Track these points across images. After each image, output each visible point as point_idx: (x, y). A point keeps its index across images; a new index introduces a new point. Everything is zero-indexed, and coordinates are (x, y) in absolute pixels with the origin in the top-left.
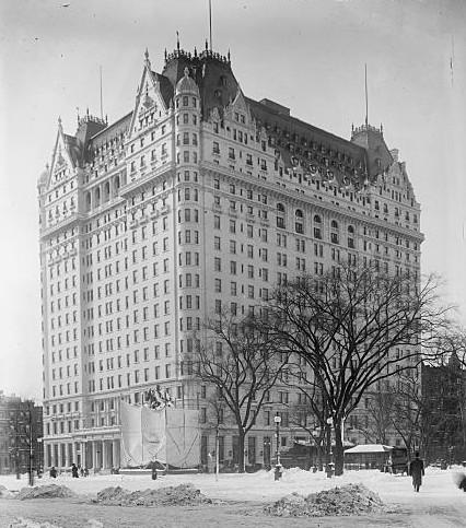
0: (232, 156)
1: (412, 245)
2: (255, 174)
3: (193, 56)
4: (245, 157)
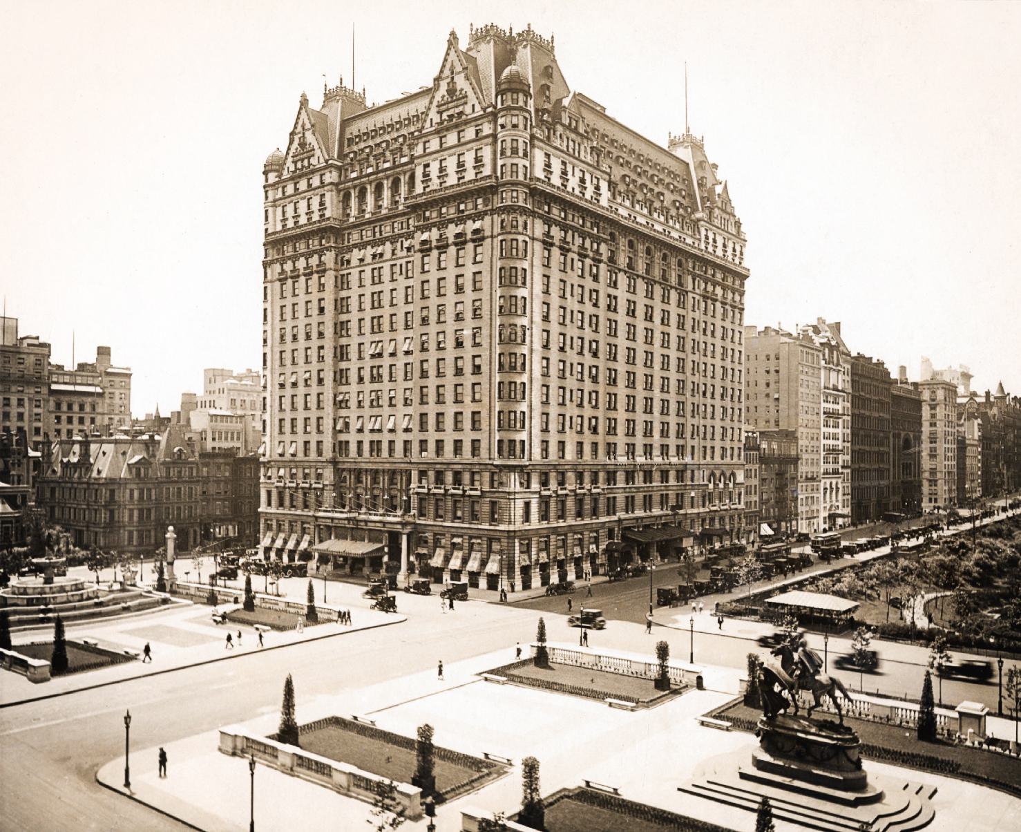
0: (564, 173)
1: (737, 282)
2: (588, 196)
3: (508, 34)
4: (578, 174)
